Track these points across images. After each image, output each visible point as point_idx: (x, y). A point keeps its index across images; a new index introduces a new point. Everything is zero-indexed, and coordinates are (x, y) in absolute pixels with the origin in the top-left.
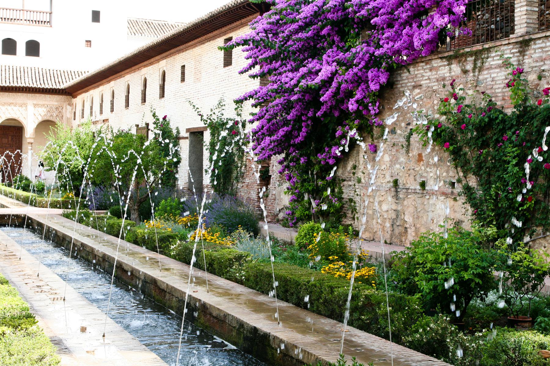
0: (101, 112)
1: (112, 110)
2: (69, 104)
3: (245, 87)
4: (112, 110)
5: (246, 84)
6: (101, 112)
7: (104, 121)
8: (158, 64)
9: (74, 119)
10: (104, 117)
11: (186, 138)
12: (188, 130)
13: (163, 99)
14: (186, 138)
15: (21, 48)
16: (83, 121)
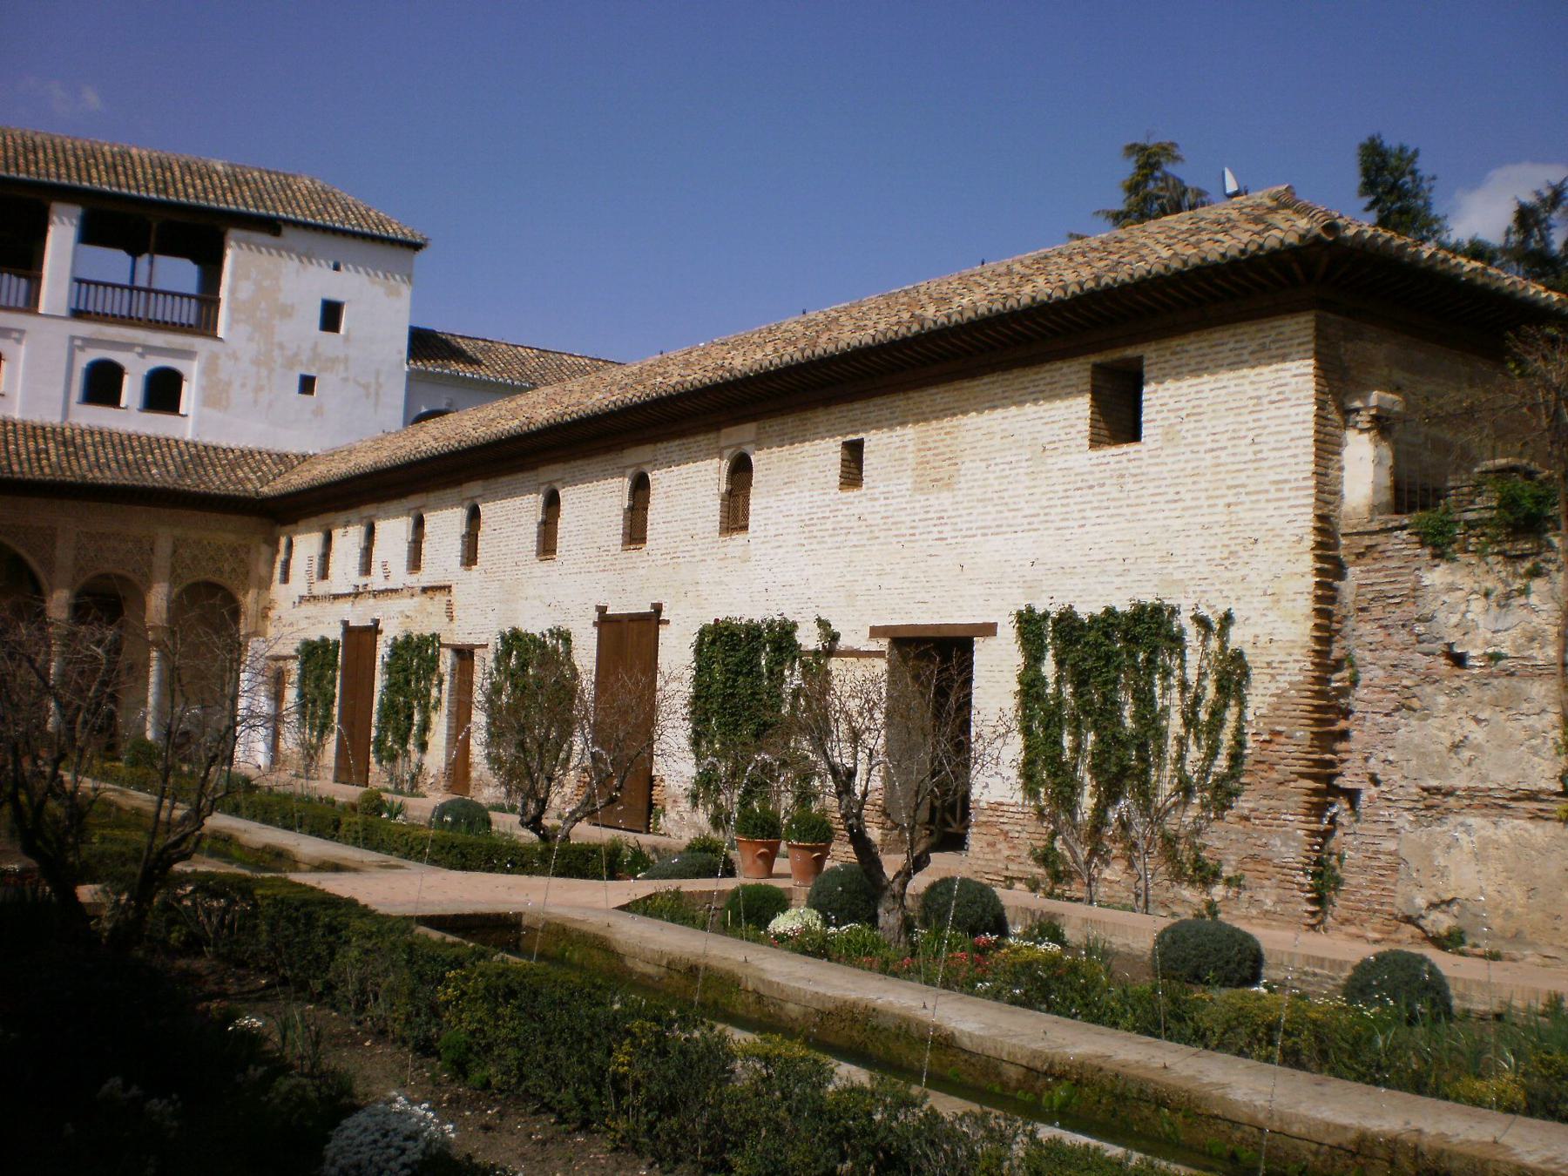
0: (415, 563)
1: (470, 557)
2: (266, 542)
3: (1220, 508)
4: (470, 557)
5: (1232, 499)
6: (415, 563)
7: (425, 590)
8: (712, 435)
9: (285, 579)
10: (426, 577)
11: (879, 654)
12: (876, 632)
13: (739, 538)
14: (879, 654)
15: (132, 390)
16: (321, 588)
